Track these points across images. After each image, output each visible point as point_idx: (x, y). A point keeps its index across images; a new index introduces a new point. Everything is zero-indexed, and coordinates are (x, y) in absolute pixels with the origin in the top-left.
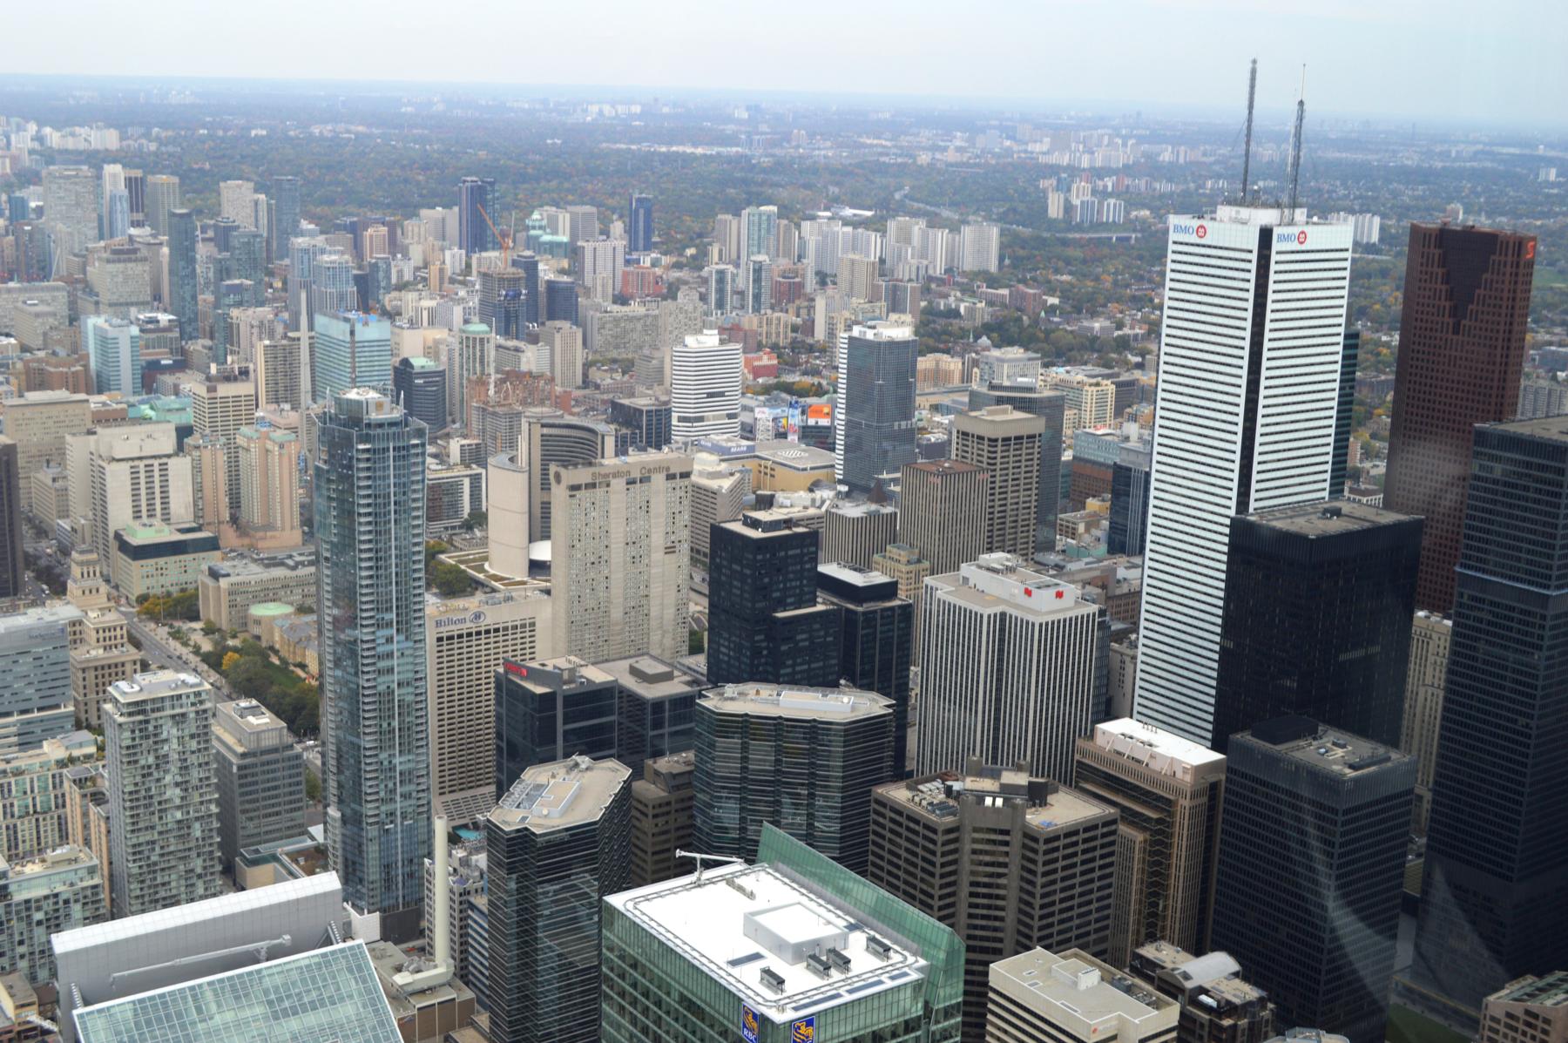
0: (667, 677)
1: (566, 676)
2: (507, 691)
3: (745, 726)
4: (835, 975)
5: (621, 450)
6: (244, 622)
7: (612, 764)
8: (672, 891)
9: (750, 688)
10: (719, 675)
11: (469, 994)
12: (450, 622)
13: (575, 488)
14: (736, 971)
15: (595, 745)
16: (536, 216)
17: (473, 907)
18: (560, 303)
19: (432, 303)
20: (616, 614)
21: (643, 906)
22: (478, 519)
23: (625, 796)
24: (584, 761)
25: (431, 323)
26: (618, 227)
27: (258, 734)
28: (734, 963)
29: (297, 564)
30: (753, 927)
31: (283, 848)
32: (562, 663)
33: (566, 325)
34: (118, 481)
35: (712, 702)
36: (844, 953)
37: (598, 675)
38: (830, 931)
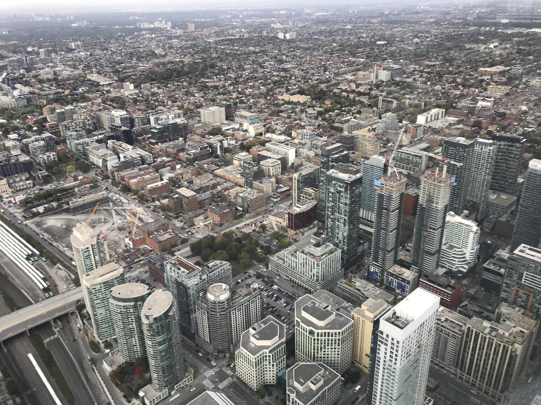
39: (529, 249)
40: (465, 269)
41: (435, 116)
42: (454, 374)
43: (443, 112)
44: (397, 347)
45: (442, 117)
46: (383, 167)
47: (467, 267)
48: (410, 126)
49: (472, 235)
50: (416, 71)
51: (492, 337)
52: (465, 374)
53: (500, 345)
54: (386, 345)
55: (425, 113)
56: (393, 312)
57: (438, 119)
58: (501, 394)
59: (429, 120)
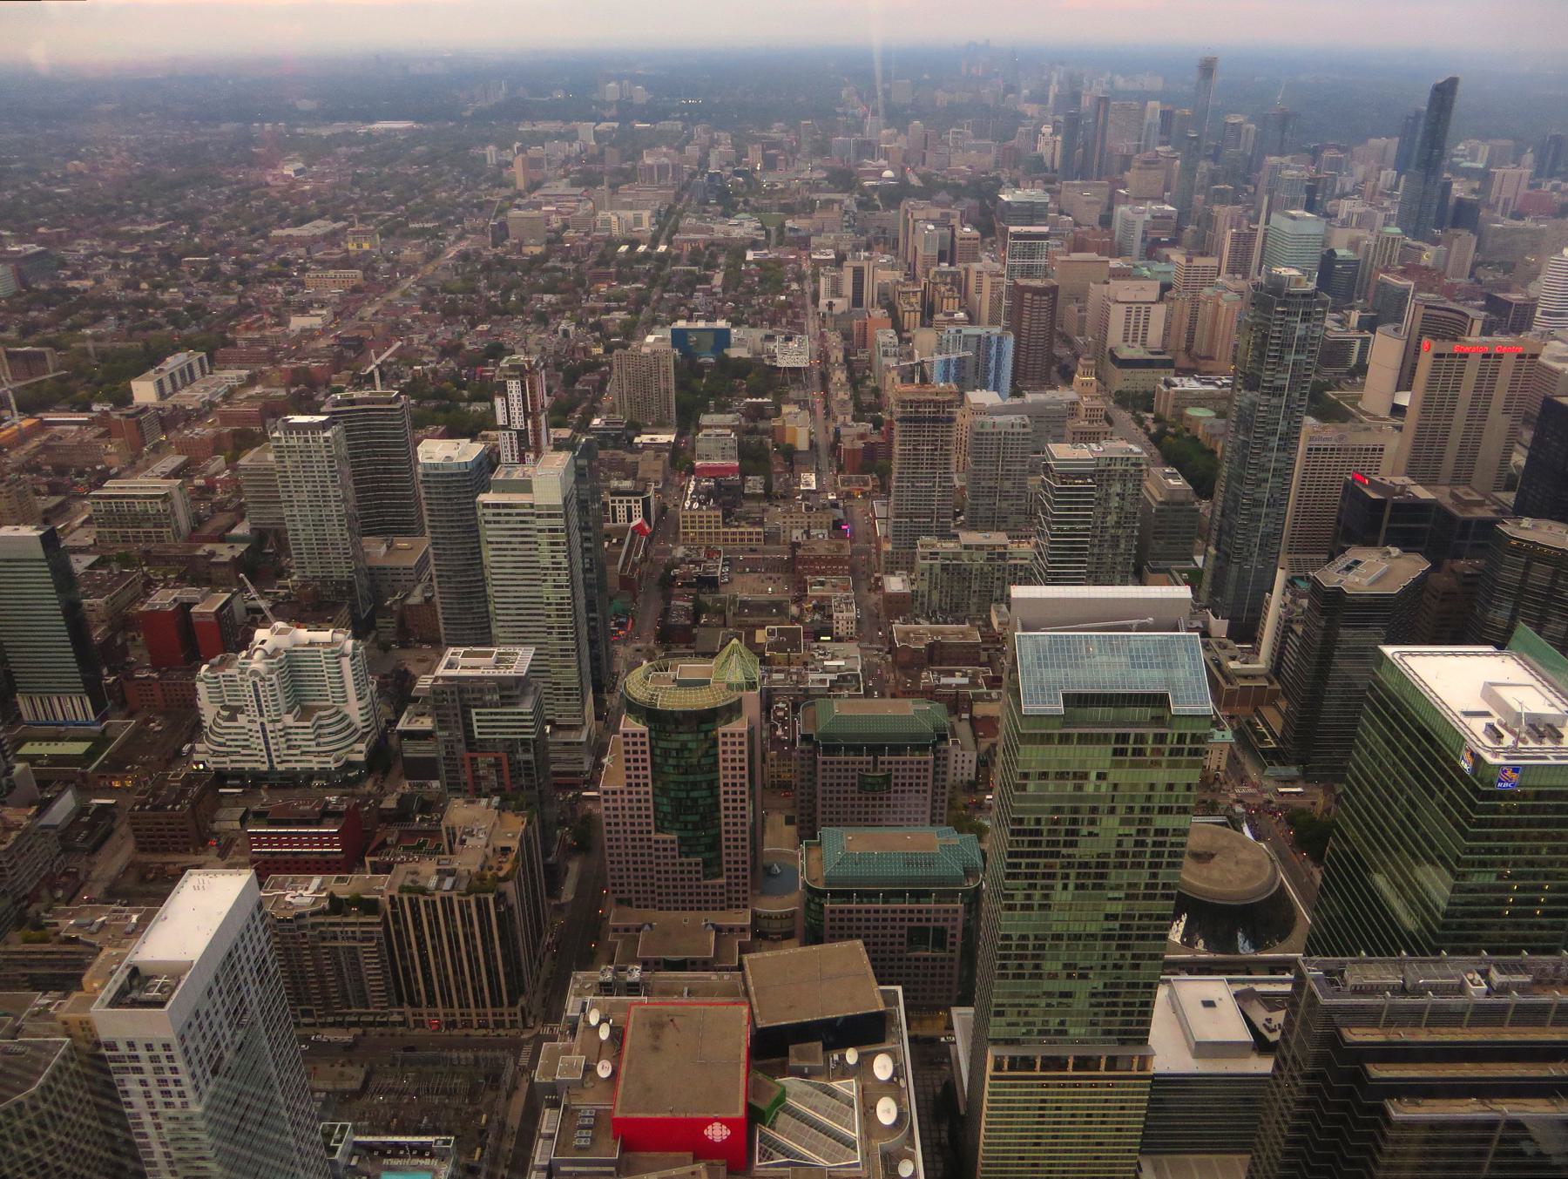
0: (1480, 504)
1: (1398, 489)
2: (1352, 492)
3: (1533, 553)
4: (1548, 743)
5: (1486, 331)
6: (1181, 416)
7: (1417, 557)
8: (1432, 654)
9: (1545, 524)
10: (1520, 510)
11: (1277, 686)
12: (1321, 439)
13: (1438, 356)
14: (1466, 720)
15: (1408, 543)
16: (1461, 147)
17: (1293, 631)
18: (1463, 216)
19: (1362, 210)
20: (1452, 450)
21: (1409, 660)
22: (1362, 369)
23: (1420, 584)
24: (1395, 551)
25: (1359, 225)
26: (1529, 158)
27: (1173, 491)
28: (1467, 714)
29: (1224, 385)
30: (1489, 690)
31: (1175, 566)
32: (1399, 480)
33: (1465, 233)
34: (1117, 315)
35: (1508, 528)
36: (1563, 731)
37: (1422, 493)
38: (1552, 711)
39: (465, 655)
40: (359, 752)
41: (182, 372)
42: (402, 1024)
43: (201, 360)
44: (170, 1058)
45: (203, 373)
46: (41, 554)
47: (362, 747)
48: (115, 416)
49: (346, 662)
50: (97, 254)
51: (446, 895)
52: (424, 1010)
53: (468, 903)
54: (139, 1070)
55: (152, 372)
56: (127, 972)
57: (193, 379)
58: (512, 1010)
59: (168, 388)
